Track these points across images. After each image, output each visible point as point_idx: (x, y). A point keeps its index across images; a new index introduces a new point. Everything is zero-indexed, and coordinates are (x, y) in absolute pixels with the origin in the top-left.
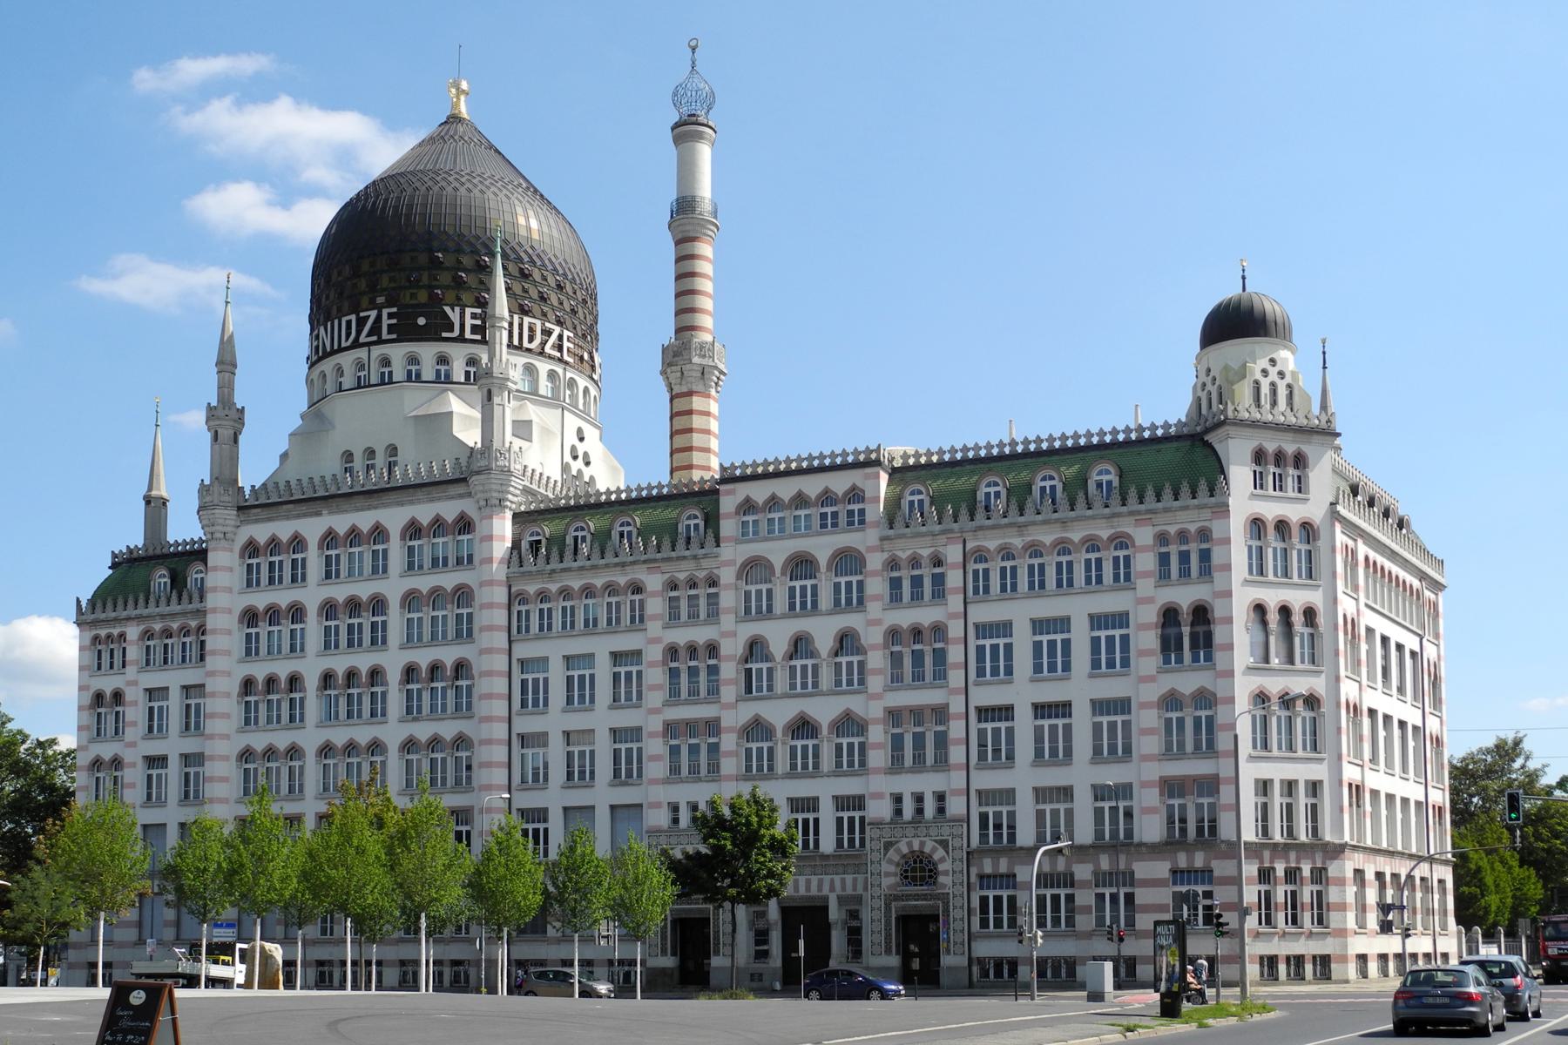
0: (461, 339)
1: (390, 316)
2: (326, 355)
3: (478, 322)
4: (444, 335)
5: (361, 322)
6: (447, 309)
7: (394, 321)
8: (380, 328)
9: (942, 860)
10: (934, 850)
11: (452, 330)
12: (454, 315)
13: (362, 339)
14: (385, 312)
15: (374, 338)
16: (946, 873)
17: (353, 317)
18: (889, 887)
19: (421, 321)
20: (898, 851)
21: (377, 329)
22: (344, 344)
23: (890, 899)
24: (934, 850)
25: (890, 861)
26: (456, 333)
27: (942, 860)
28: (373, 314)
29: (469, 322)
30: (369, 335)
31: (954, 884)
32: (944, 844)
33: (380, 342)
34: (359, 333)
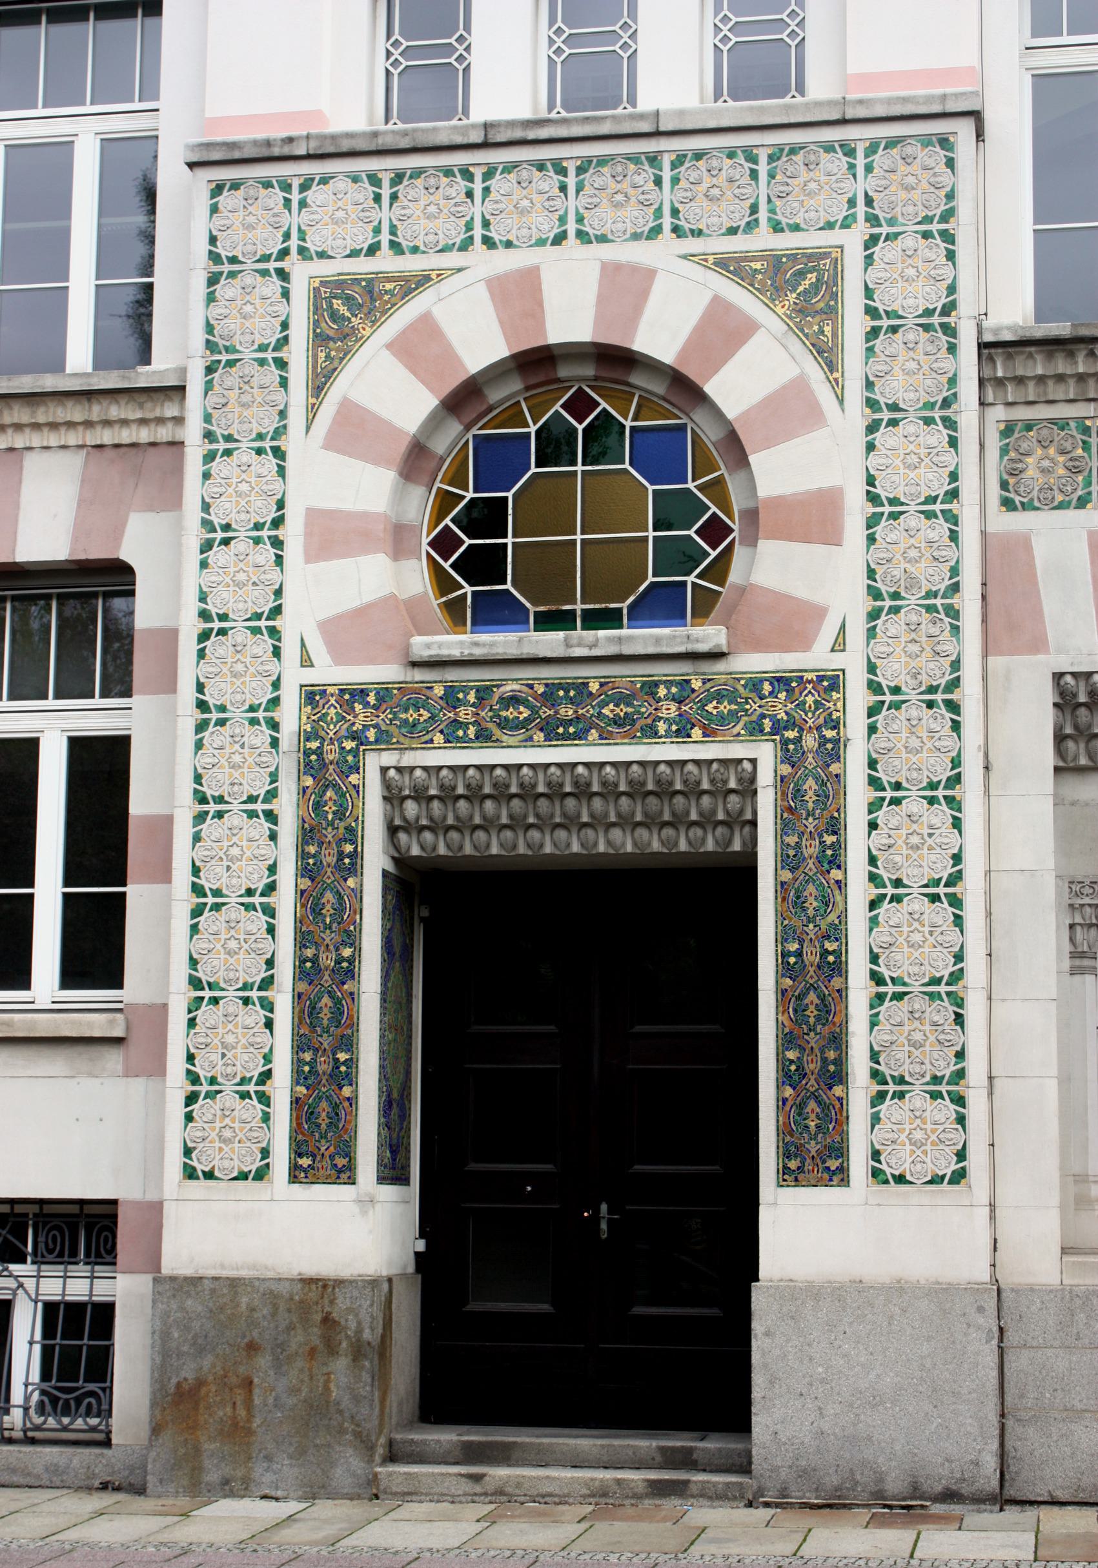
9: (791, 411)
10: (722, 333)
16: (814, 519)
18: (344, 632)
20: (421, 348)
23: (336, 733)
24: (722, 333)
25: (355, 432)
27: (791, 411)
31: (882, 602)
32: (803, 288)
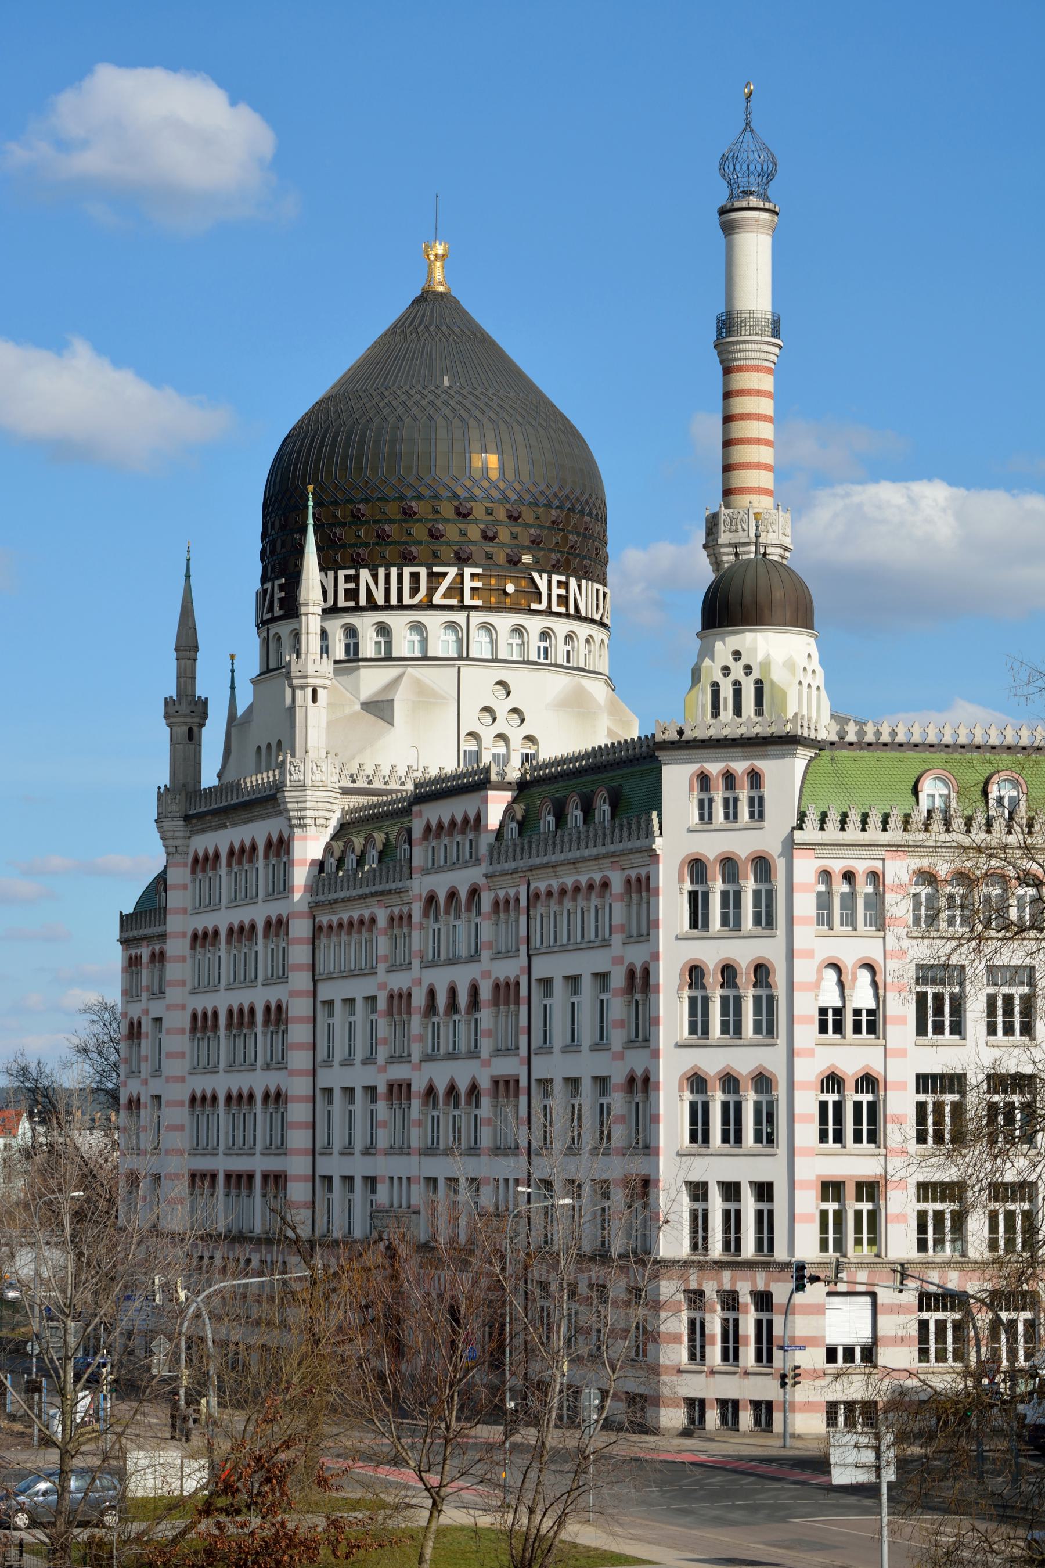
0: (549, 612)
1: (473, 575)
2: (373, 606)
3: (563, 592)
4: (534, 606)
5: (435, 578)
6: (536, 575)
7: (479, 584)
8: (462, 590)
11: (540, 602)
12: (542, 583)
13: (437, 599)
14: (468, 571)
15: (454, 602)
17: (423, 571)
19: (510, 588)
21: (456, 589)
22: (407, 600)
26: (543, 606)
28: (452, 572)
29: (556, 591)
30: (445, 596)
33: (462, 607)
34: (431, 591)
